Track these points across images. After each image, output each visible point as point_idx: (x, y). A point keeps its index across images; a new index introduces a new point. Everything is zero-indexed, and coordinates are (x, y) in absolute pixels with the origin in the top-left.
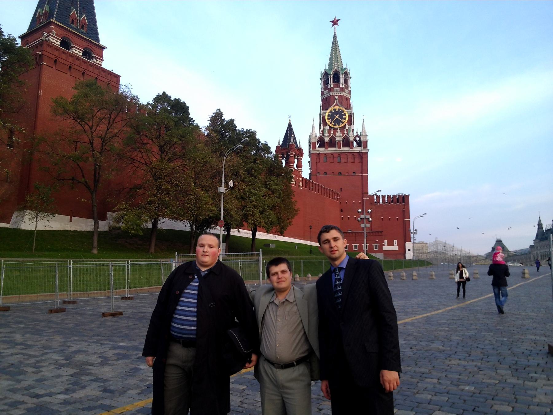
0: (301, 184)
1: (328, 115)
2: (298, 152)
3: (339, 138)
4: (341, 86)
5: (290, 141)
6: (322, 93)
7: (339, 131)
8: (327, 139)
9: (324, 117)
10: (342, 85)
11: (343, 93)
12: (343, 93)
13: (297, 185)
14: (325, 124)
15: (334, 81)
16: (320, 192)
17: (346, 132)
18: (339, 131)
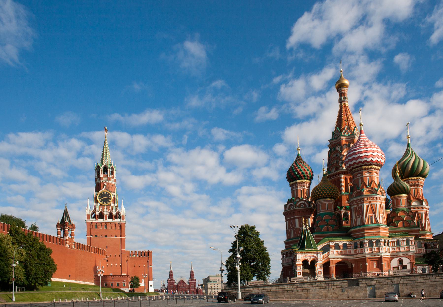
0: (73, 247)
1: (99, 196)
2: (71, 227)
3: (106, 213)
4: (108, 176)
5: (65, 220)
6: (96, 179)
7: (105, 208)
8: (97, 213)
9: (96, 197)
10: (110, 176)
11: (110, 182)
12: (110, 182)
13: (71, 247)
14: (97, 202)
15: (104, 173)
16: (88, 250)
17: (110, 209)
18: (105, 208)
